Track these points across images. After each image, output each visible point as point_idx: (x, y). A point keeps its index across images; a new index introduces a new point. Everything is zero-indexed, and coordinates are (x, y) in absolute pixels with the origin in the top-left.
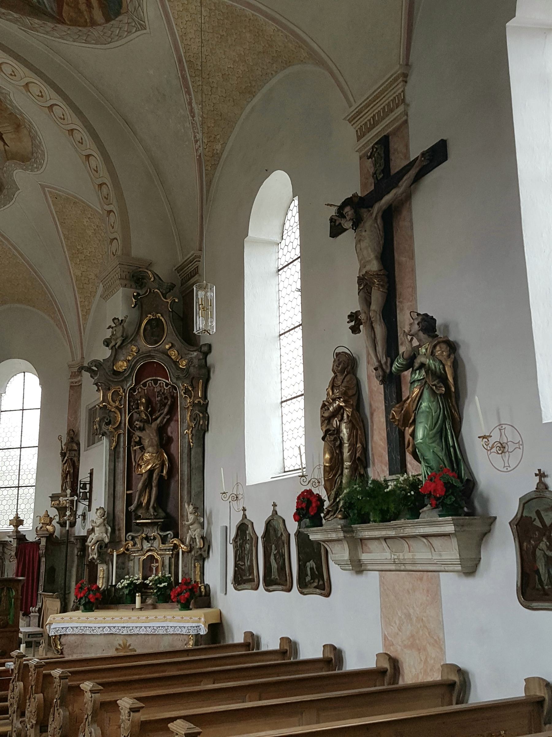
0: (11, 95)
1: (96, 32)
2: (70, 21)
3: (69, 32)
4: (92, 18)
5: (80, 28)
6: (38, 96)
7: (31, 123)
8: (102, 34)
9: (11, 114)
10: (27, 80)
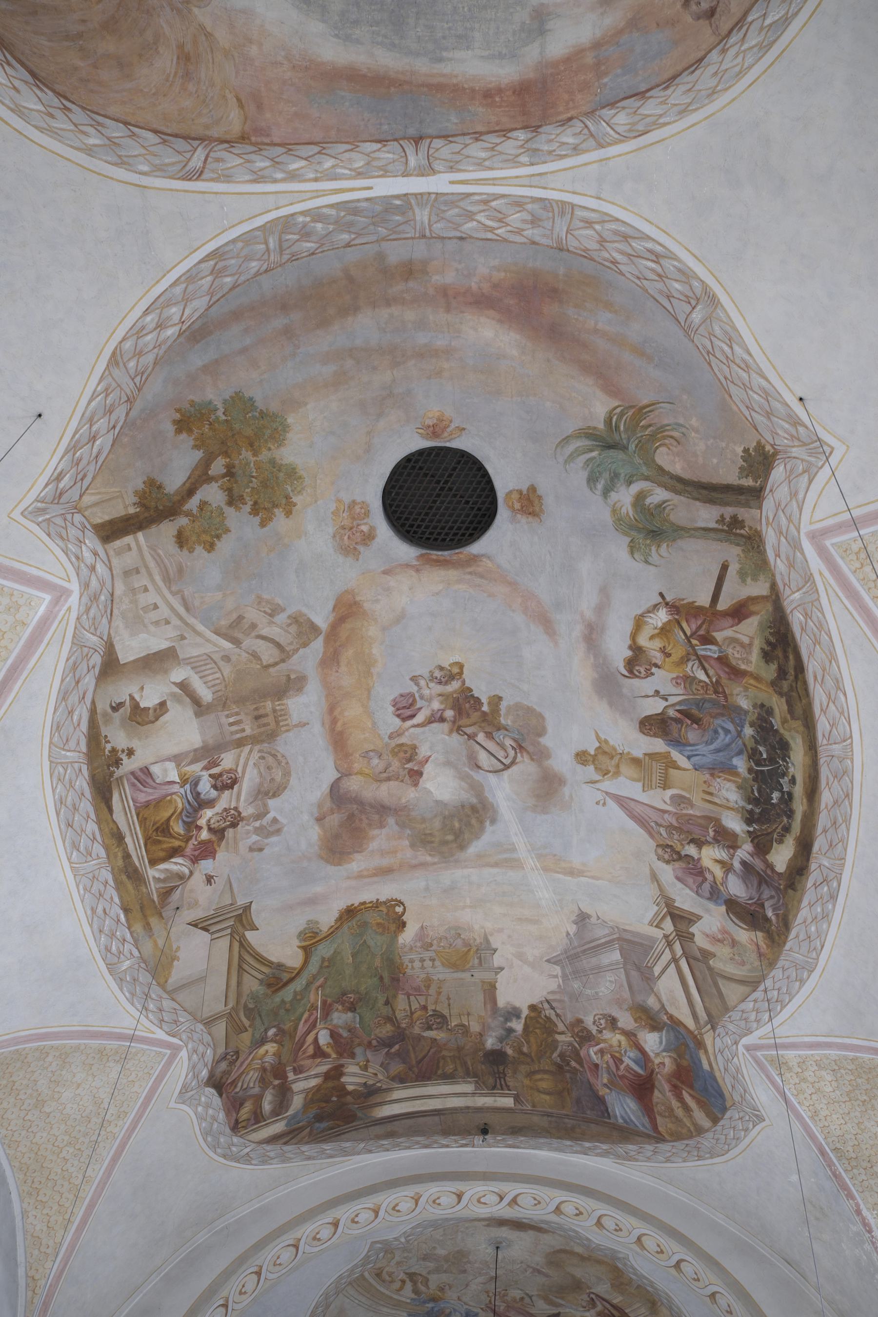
0: (631, 1258)
1: (706, 1141)
2: (671, 1135)
3: (674, 1151)
4: (695, 1125)
5: (686, 1142)
6: (657, 1252)
7: (669, 1297)
8: (714, 1142)
9: (639, 1287)
10: (636, 1233)
